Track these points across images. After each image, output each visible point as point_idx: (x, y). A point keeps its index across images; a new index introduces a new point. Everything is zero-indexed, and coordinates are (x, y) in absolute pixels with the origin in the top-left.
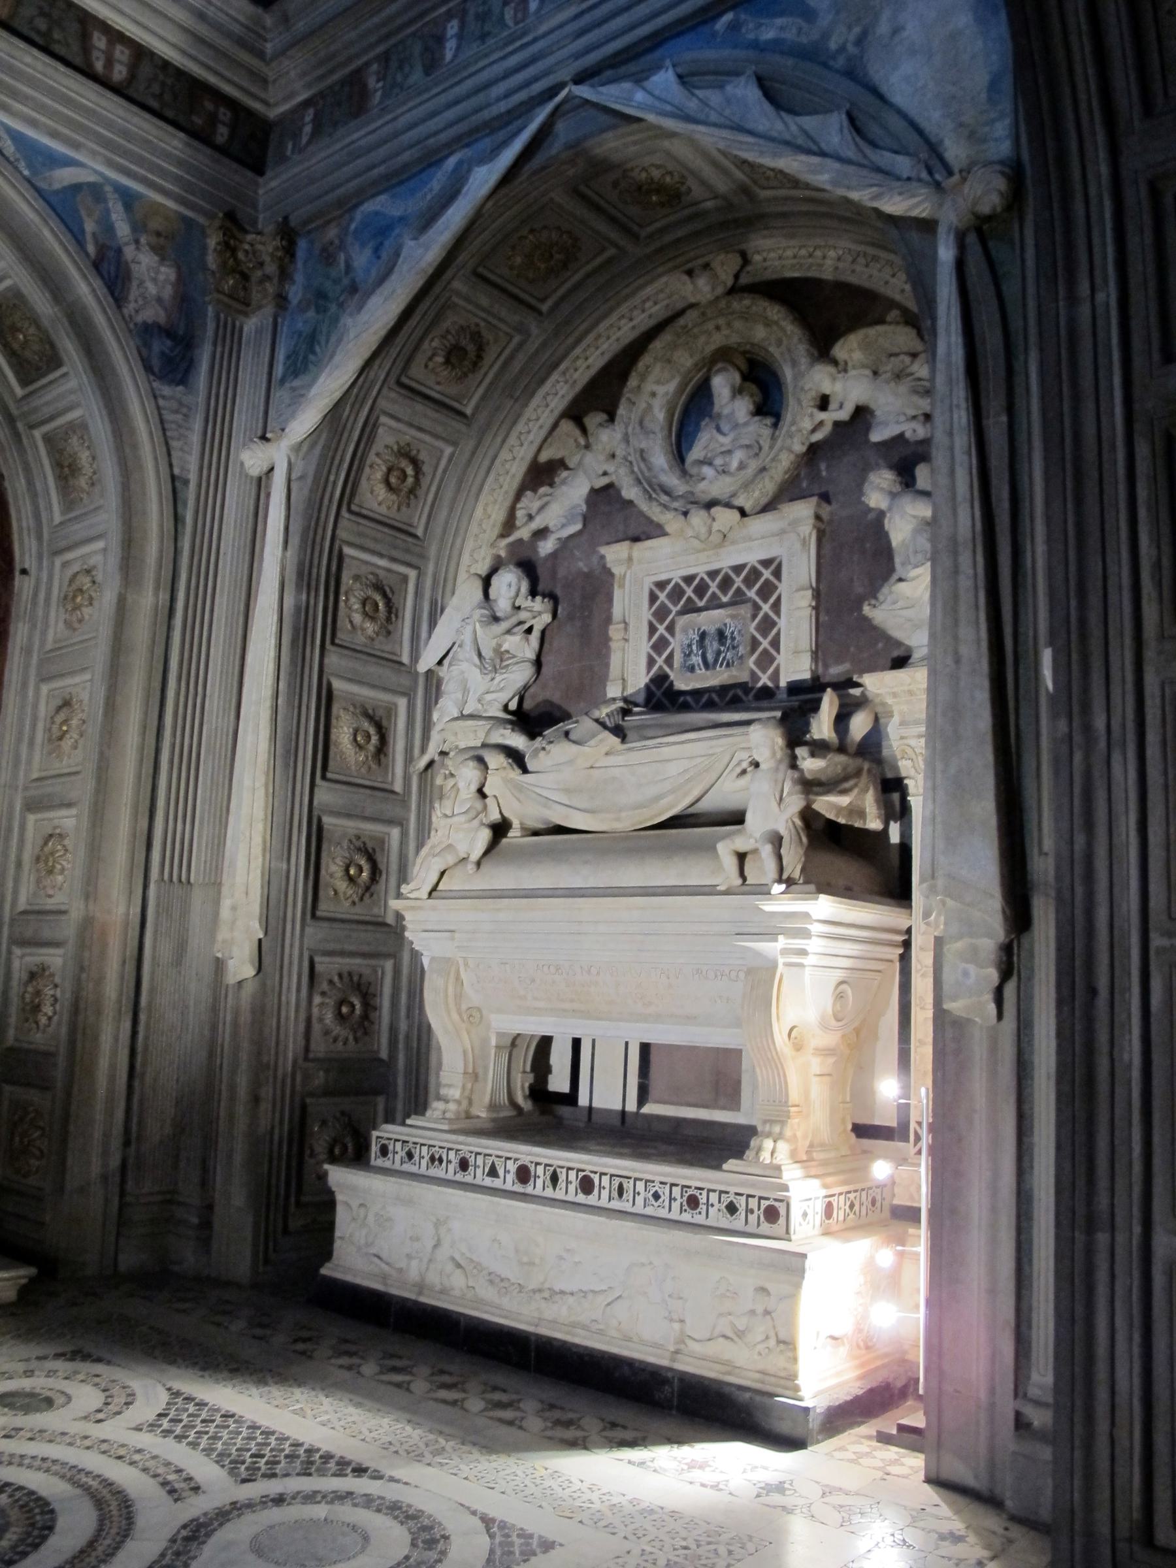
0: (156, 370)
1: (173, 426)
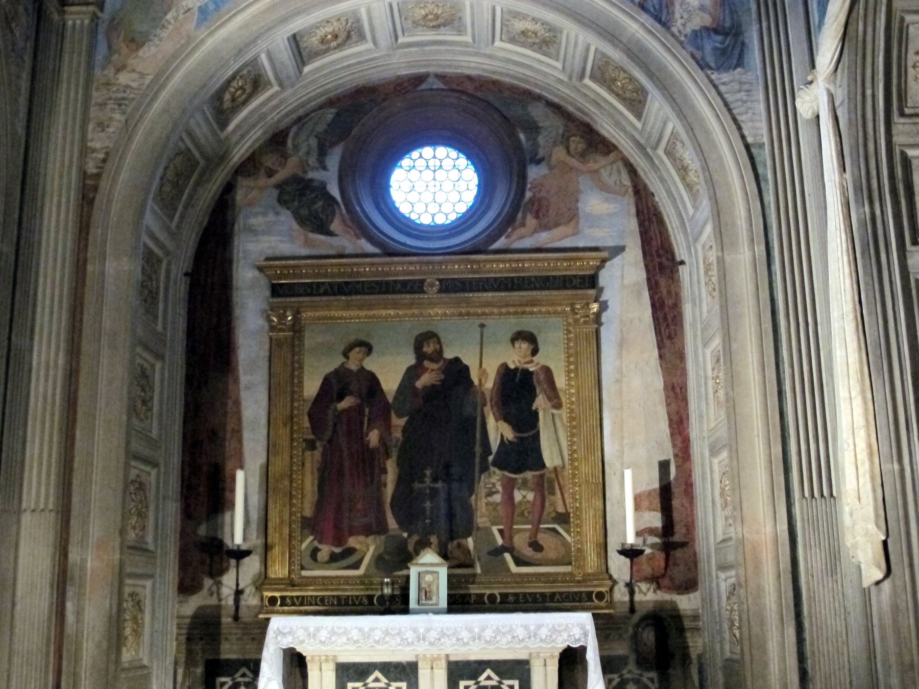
0: (712, 65)
1: (740, 103)
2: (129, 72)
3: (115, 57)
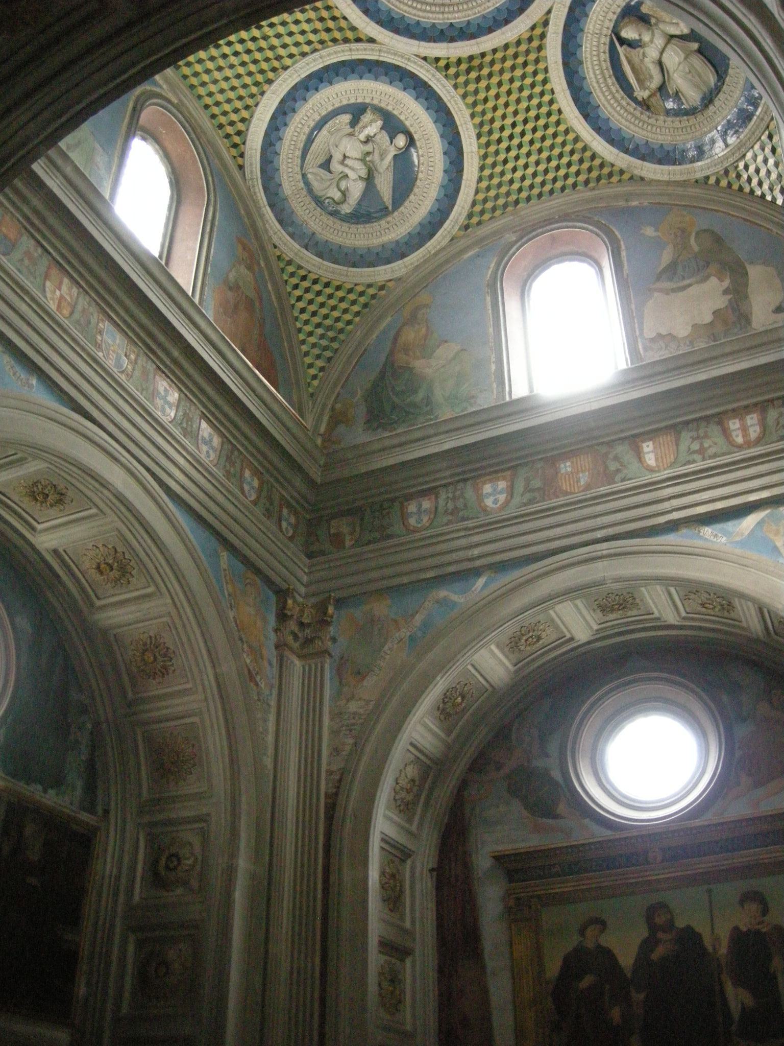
2: (357, 700)
3: (345, 689)
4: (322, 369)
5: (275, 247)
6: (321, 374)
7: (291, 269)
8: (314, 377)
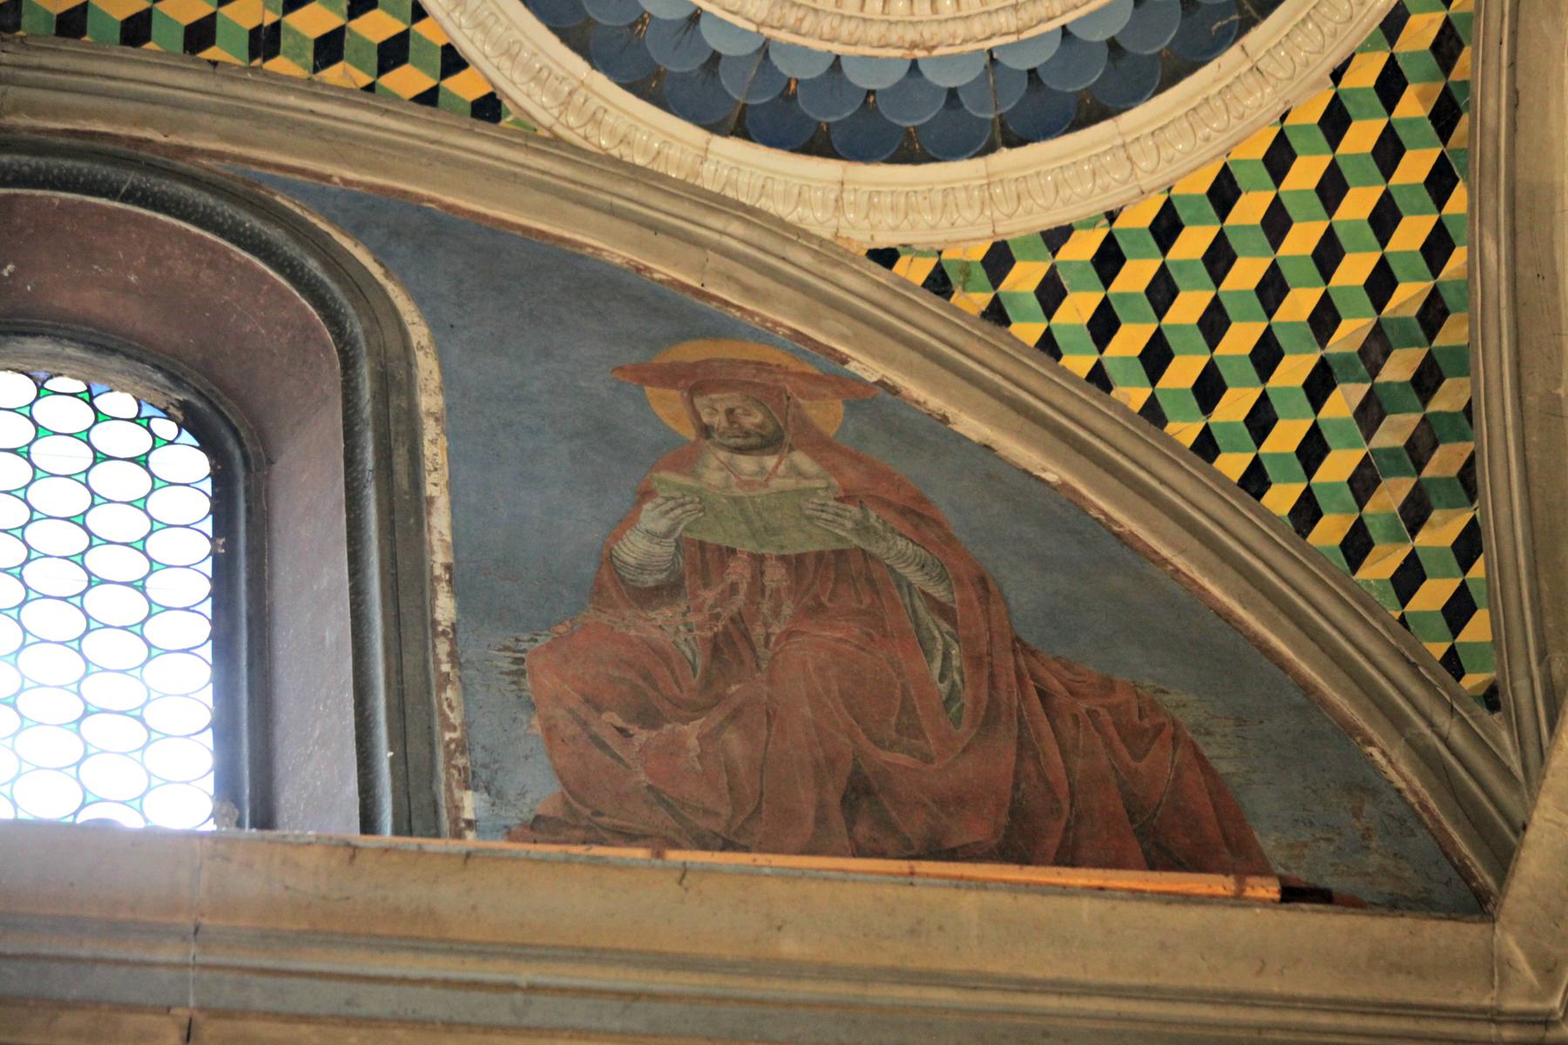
4: (1468, 547)
5: (886, 257)
6: (1478, 570)
7: (1024, 278)
8: (1459, 610)
